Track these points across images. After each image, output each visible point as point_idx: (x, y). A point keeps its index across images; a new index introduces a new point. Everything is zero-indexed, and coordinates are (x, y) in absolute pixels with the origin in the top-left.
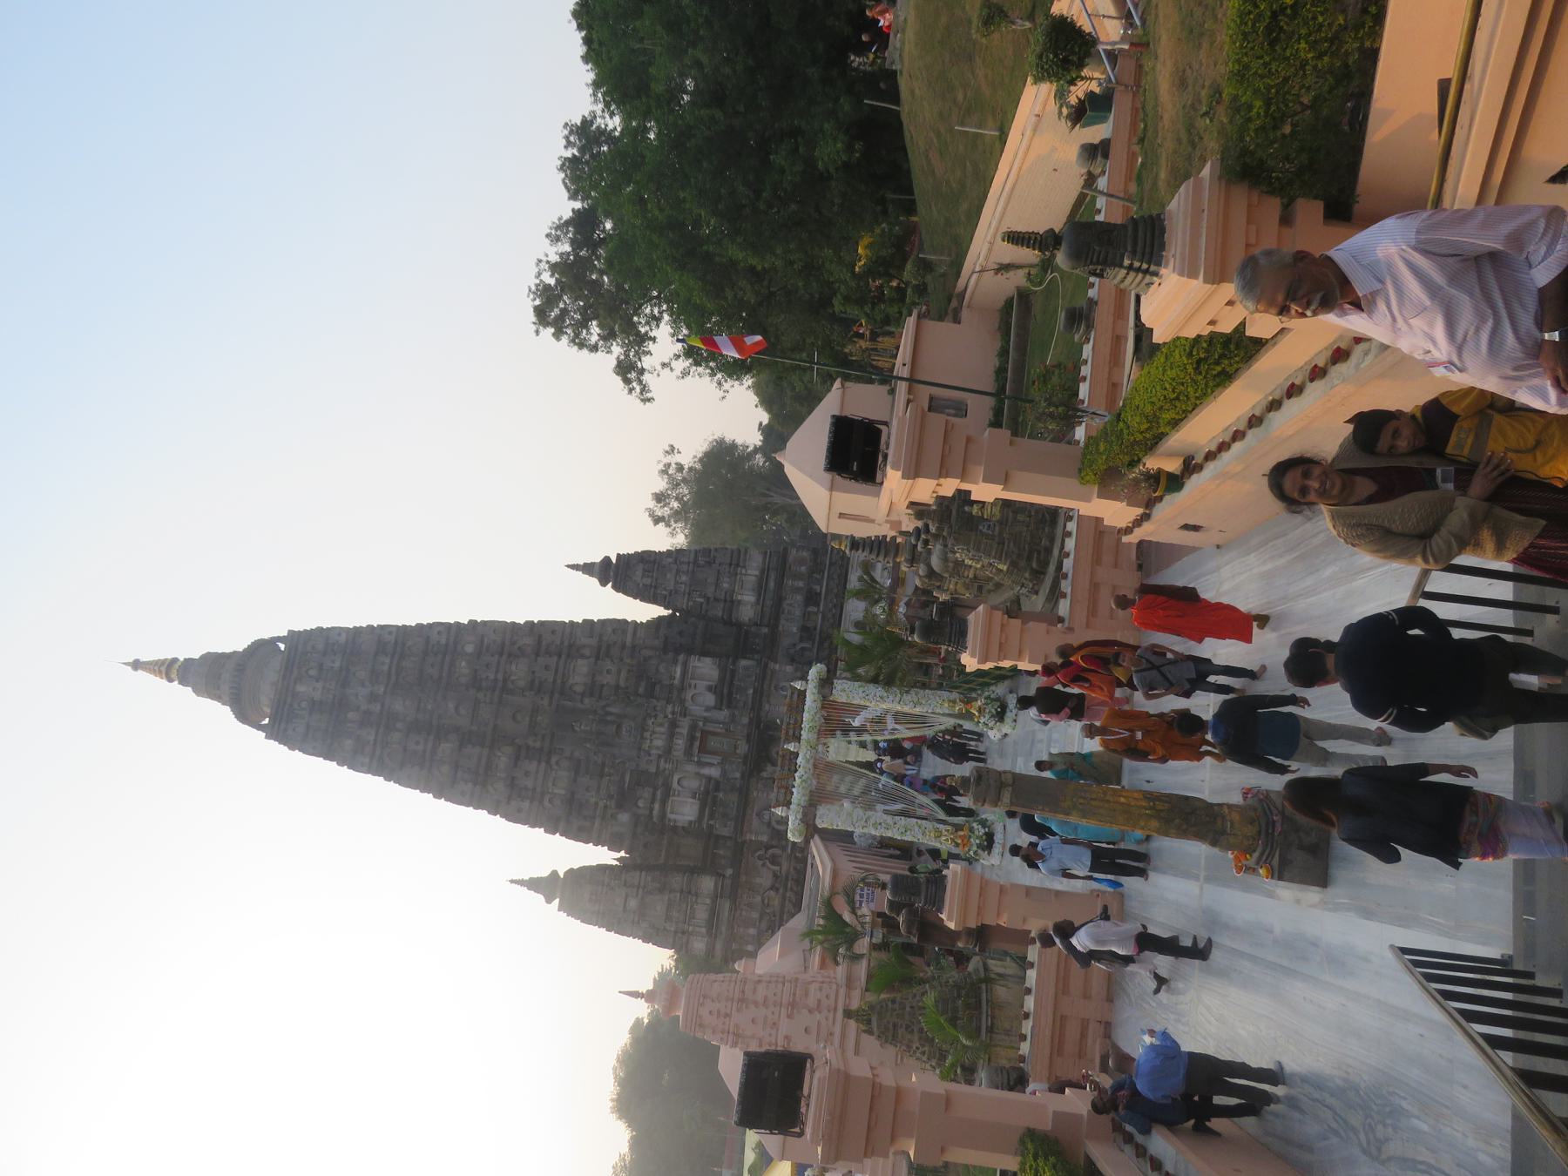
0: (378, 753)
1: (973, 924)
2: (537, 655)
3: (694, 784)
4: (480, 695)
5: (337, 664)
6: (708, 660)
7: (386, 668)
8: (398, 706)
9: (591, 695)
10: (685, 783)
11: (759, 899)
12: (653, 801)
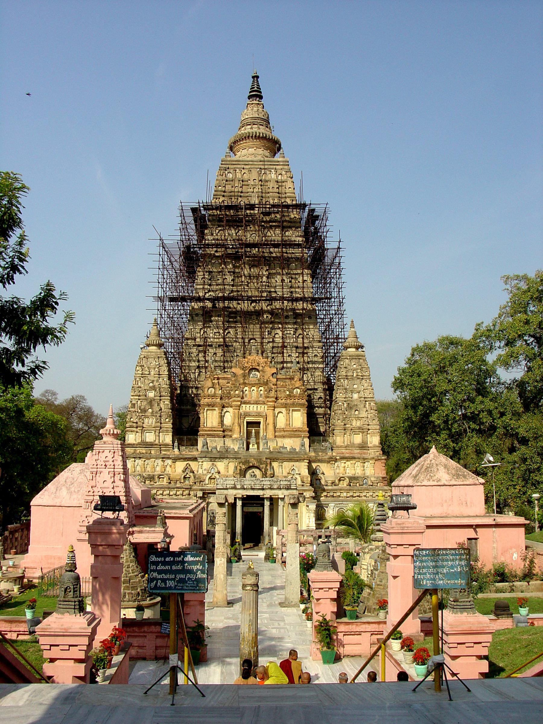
4: (265, 279)
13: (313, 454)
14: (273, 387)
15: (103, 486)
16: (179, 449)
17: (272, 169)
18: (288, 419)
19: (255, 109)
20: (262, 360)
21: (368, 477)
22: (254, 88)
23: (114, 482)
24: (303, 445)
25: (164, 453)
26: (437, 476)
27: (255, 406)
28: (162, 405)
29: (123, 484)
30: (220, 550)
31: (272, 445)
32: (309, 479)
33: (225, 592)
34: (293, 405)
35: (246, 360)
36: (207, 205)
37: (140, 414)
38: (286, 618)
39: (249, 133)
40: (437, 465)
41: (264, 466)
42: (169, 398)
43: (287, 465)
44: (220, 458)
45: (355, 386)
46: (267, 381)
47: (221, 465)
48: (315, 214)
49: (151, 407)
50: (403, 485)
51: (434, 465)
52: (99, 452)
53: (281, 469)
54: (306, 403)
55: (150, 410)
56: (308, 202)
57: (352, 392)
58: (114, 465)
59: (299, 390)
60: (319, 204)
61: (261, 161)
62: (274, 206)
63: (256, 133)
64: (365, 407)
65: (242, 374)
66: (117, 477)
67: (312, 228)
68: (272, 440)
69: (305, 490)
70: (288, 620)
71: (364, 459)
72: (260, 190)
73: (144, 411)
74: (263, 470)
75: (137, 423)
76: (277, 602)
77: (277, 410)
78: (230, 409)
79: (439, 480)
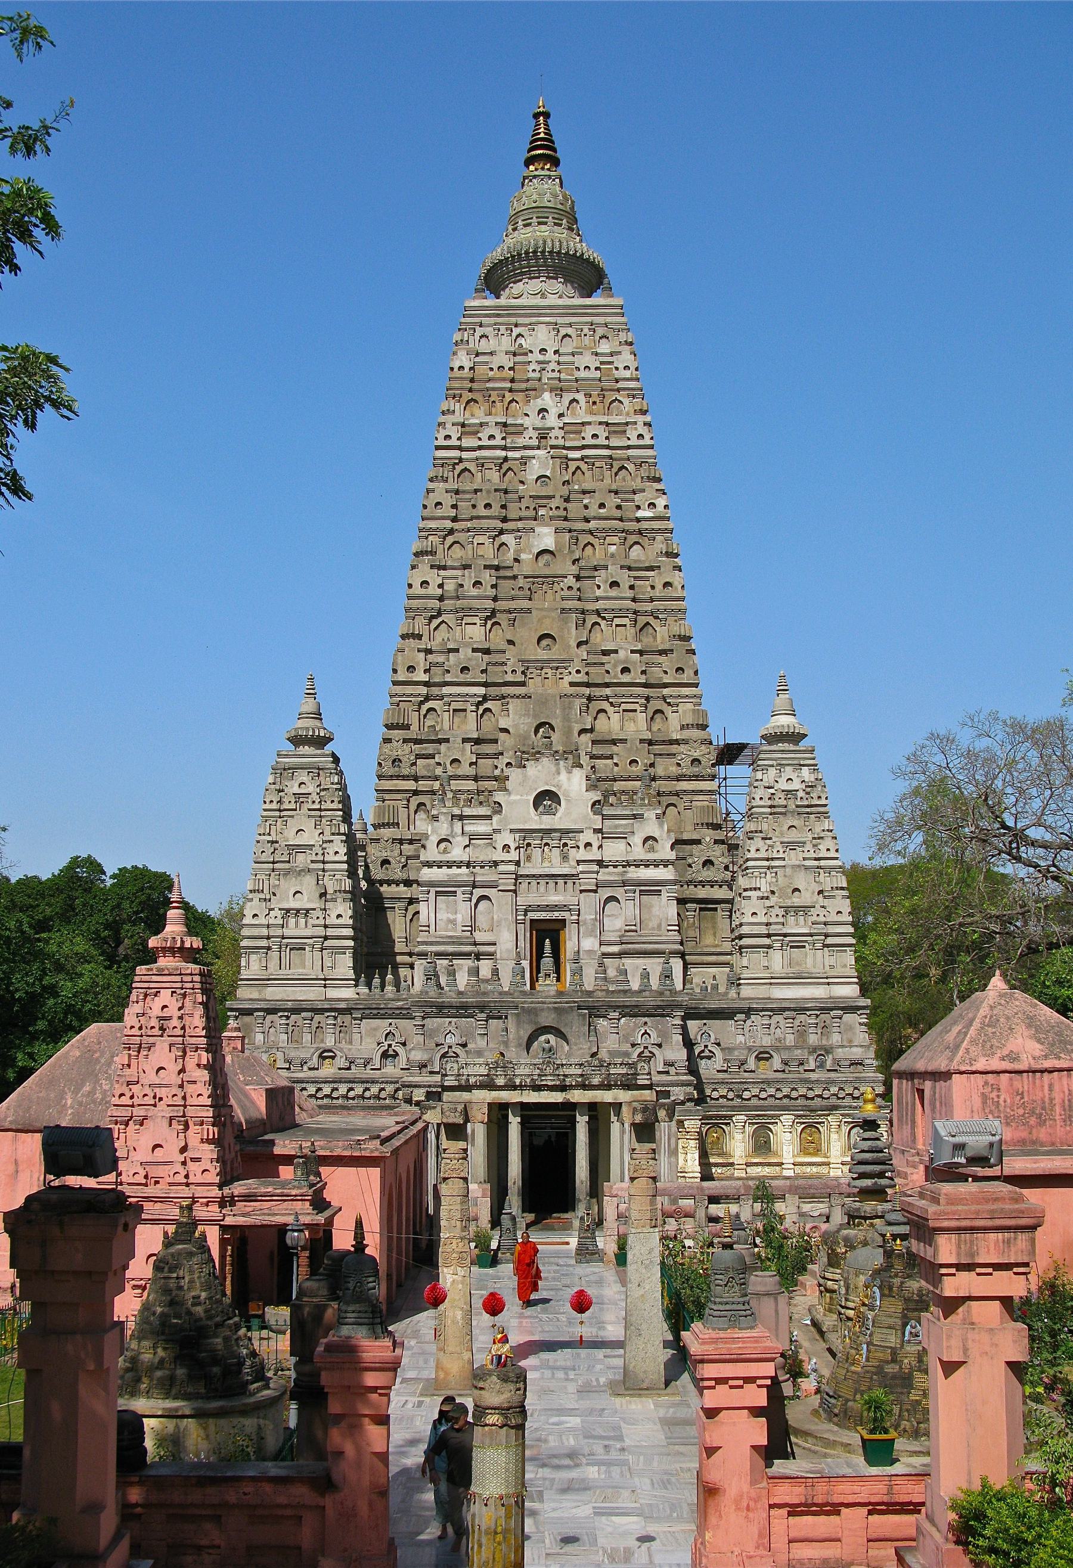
0: (465, 455)
1: (325, 1379)
2: (641, 653)
3: (482, 921)
4: (571, 581)
5: (583, 374)
6: (673, 909)
7: (589, 441)
8: (535, 469)
9: (594, 742)
10: (483, 904)
11: (329, 1042)
12: (450, 865)
22: (539, 134)
23: (182, 1071)
29: (204, 1075)
30: (454, 1246)
33: (467, 1355)
38: (626, 1429)
40: (1008, 1018)
42: (345, 866)
52: (146, 995)
58: (183, 1028)
63: (545, 242)
66: (191, 1061)
70: (633, 1436)
76: (602, 1380)
79: (1013, 1057)
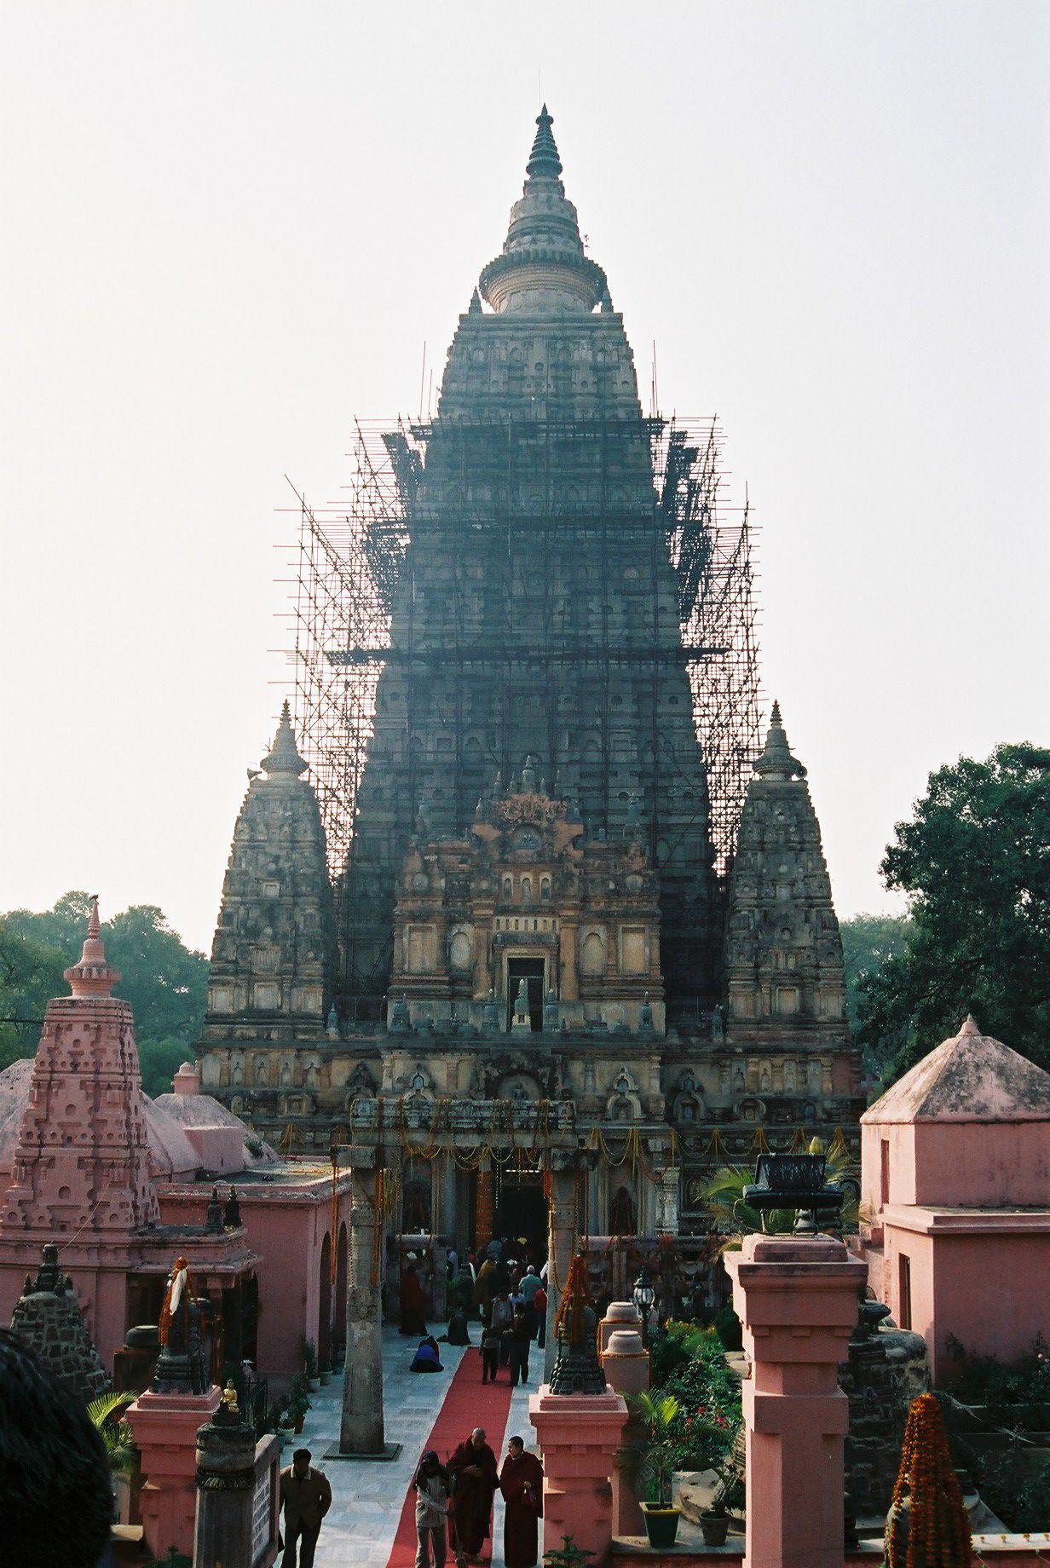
13: (675, 1040)
14: (576, 871)
15: (65, 1119)
16: (339, 1026)
17: (583, 337)
18: (613, 950)
19: (543, 196)
20: (548, 805)
21: (816, 1100)
24: (647, 1018)
25: (301, 1037)
26: (976, 1097)
27: (531, 920)
28: (300, 919)
31: (571, 1018)
32: (663, 1105)
34: (627, 915)
35: (508, 803)
36: (422, 427)
37: (244, 941)
39: (528, 253)
40: (977, 1066)
41: (547, 1070)
43: (605, 1068)
44: (435, 1051)
45: (783, 869)
46: (561, 855)
47: (439, 1069)
48: (688, 444)
49: (272, 919)
50: (886, 1119)
51: (971, 1068)
53: (592, 1079)
54: (658, 912)
55: (269, 931)
56: (666, 416)
57: (774, 882)
59: (639, 880)
60: (696, 419)
61: (554, 320)
62: (584, 426)
64: (807, 920)
65: (499, 838)
67: (683, 489)
68: (571, 1006)
69: (652, 1134)
71: (806, 1053)
72: (552, 390)
73: (255, 932)
74: (545, 1081)
75: (235, 962)
77: (586, 930)
78: (468, 928)
79: (983, 1108)
